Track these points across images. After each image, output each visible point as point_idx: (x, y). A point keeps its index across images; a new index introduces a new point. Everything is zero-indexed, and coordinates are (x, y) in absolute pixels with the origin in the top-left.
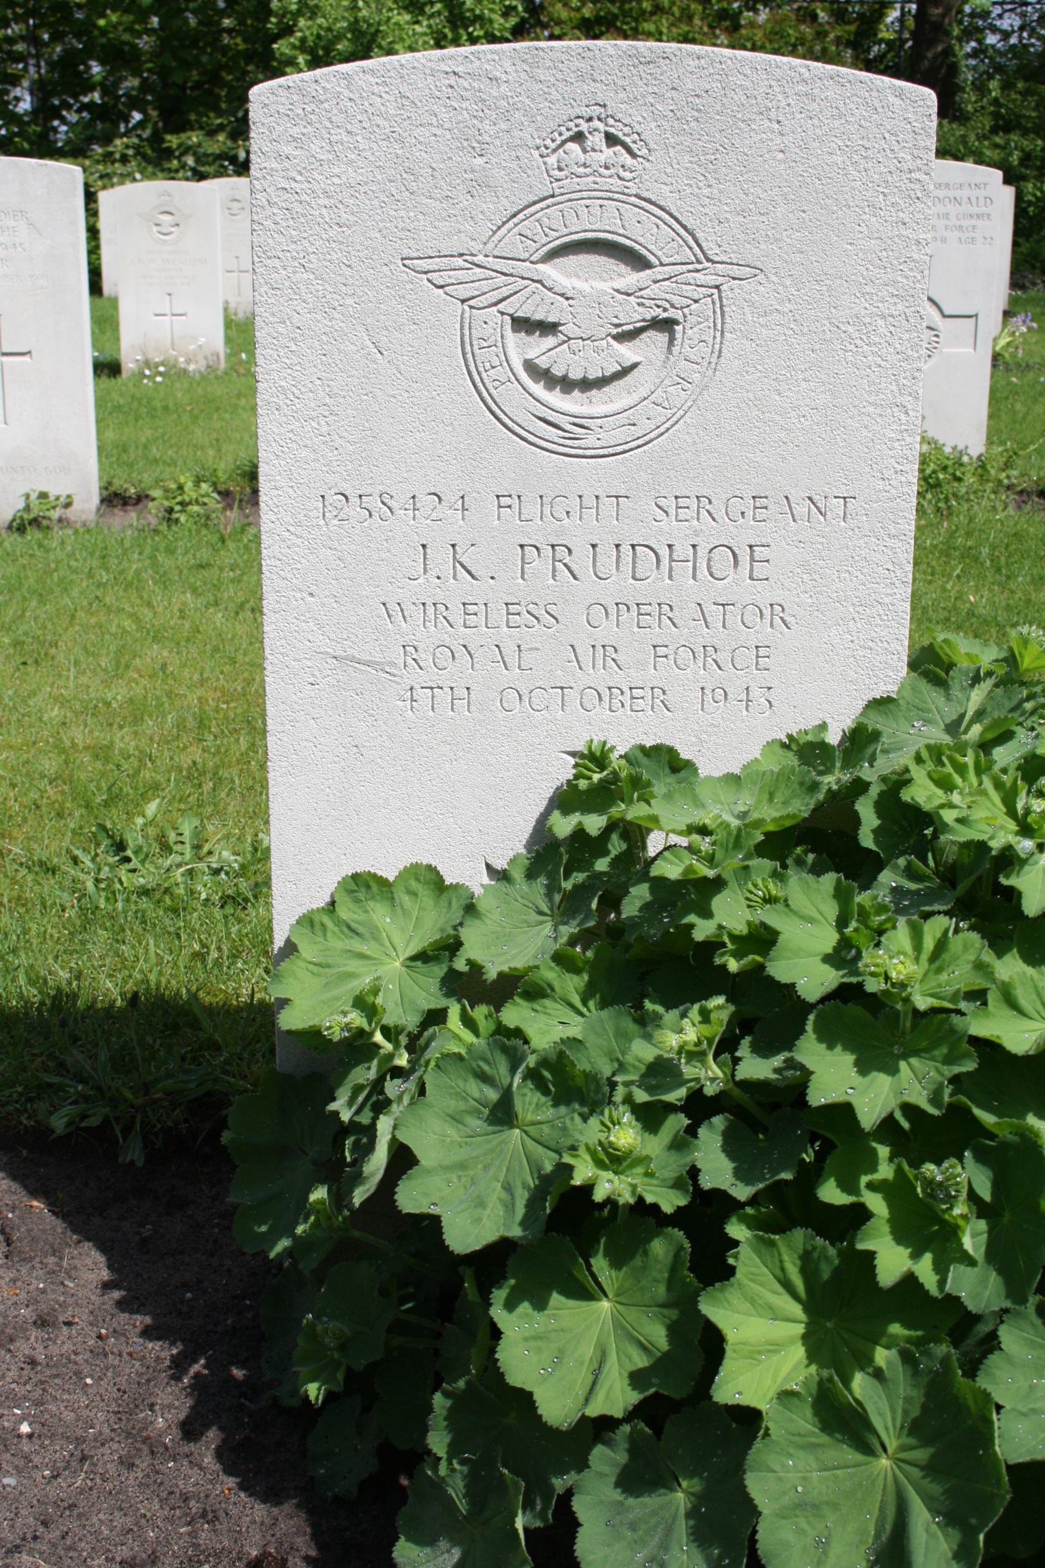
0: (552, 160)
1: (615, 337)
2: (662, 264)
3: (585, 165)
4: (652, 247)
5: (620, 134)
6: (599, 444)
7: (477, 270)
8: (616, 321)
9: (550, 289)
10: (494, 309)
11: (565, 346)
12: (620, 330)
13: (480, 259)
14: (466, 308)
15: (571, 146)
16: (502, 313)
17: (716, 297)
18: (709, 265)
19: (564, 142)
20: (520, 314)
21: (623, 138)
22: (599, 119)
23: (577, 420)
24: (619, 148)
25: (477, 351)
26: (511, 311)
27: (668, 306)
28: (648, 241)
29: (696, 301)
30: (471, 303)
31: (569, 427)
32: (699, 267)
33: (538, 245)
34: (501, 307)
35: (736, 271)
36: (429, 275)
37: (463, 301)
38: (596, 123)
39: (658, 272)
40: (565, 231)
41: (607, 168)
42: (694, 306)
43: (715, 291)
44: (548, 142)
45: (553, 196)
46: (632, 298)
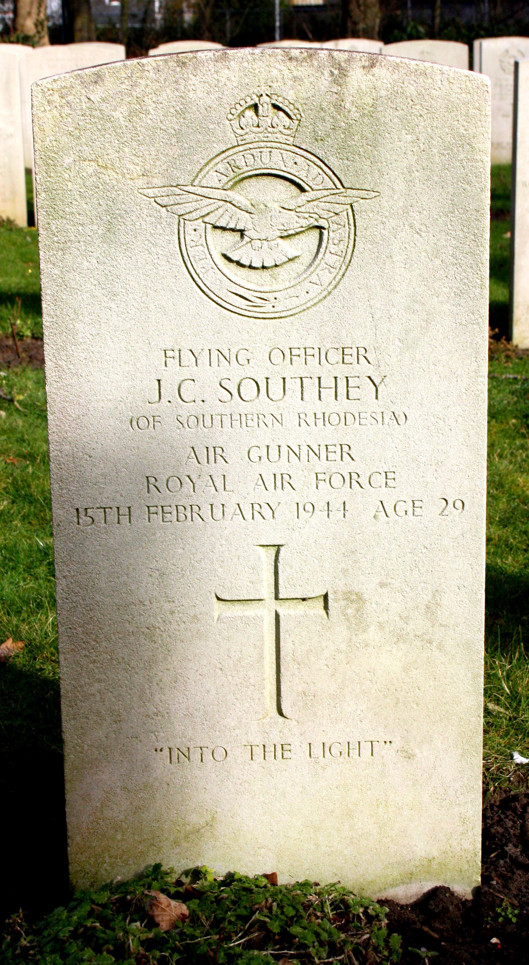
4: (305, 179)
5: (281, 105)
9: (239, 208)
10: (200, 221)
17: (350, 211)
18: (343, 190)
19: (243, 111)
20: (218, 224)
22: (267, 95)
23: (259, 295)
24: (281, 114)
27: (317, 217)
28: (303, 175)
29: (336, 214)
30: (184, 217)
32: (338, 191)
34: (206, 219)
35: (363, 194)
36: (156, 199)
38: (265, 98)
39: (310, 195)
40: (246, 169)
43: (348, 207)
44: (233, 111)
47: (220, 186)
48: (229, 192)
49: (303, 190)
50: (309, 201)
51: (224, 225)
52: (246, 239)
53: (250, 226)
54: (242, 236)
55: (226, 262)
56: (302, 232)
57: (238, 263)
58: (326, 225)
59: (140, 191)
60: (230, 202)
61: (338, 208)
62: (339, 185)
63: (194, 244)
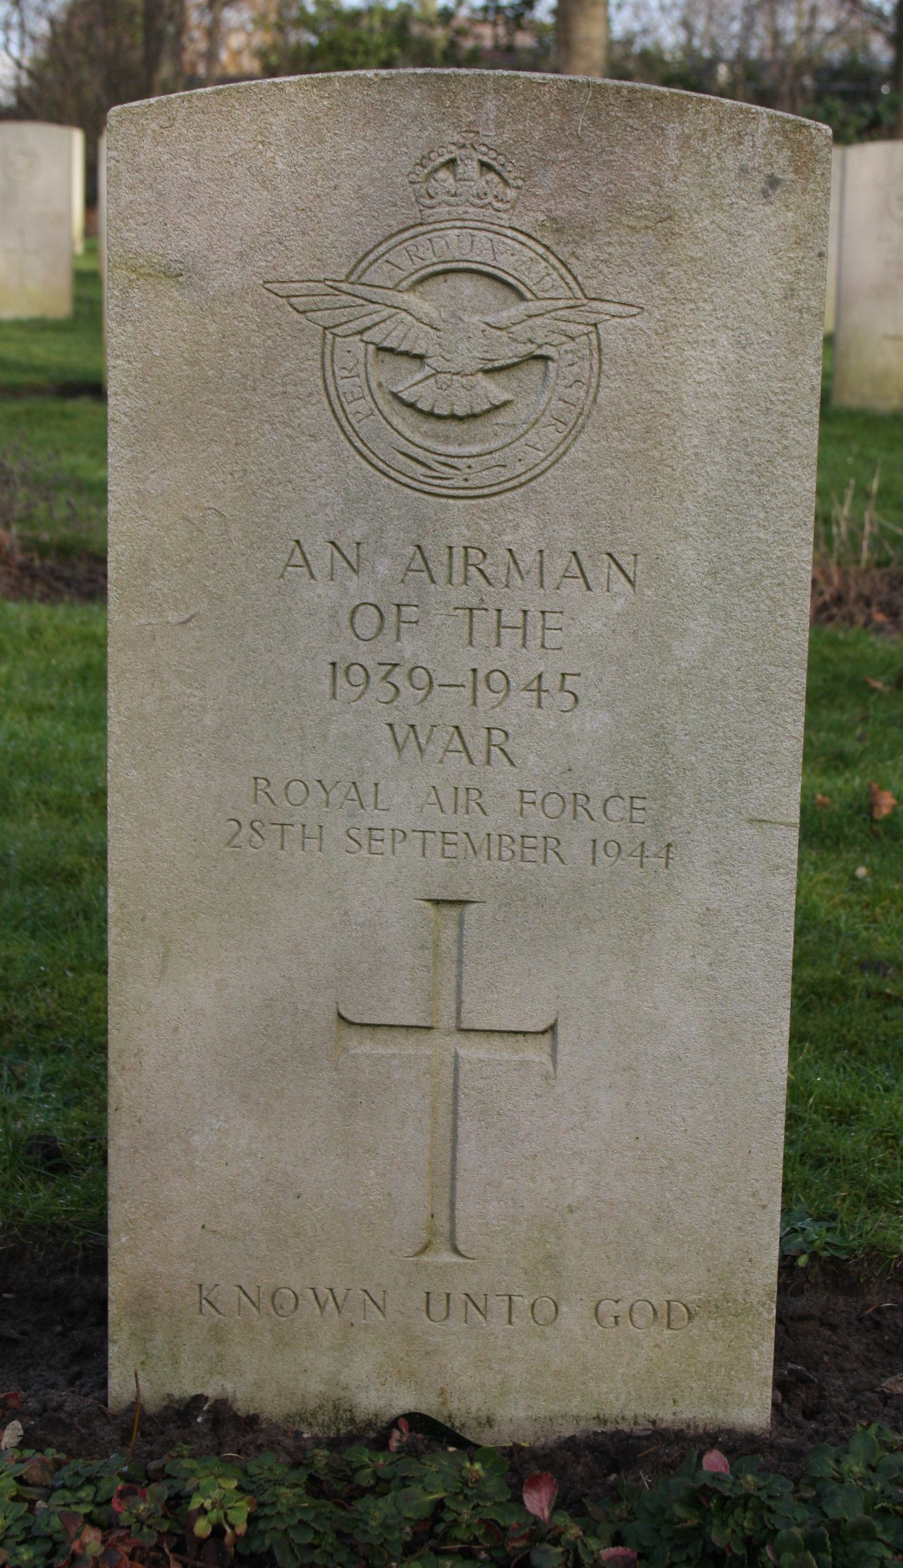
0: (421, 188)
1: (486, 372)
2: (538, 299)
3: (455, 195)
6: (467, 484)
7: (344, 297)
8: (488, 356)
10: (358, 337)
11: (432, 380)
12: (490, 366)
13: (344, 286)
14: (330, 336)
15: (442, 174)
16: (367, 343)
17: (593, 337)
18: (585, 301)
20: (385, 344)
21: (498, 168)
23: (442, 459)
25: (340, 382)
26: (377, 340)
30: (334, 331)
31: (435, 465)
33: (405, 274)
37: (326, 328)
39: (534, 307)
41: (479, 197)
42: (572, 344)
43: (591, 328)
45: (421, 224)
46: (504, 333)
47: (390, 284)
48: (405, 296)
49: (522, 297)
50: (530, 316)
51: (394, 345)
52: (428, 371)
53: (434, 350)
54: (423, 364)
55: (396, 405)
56: (514, 365)
57: (411, 406)
58: (556, 357)
59: (267, 286)
60: (405, 310)
61: (572, 328)
62: (579, 294)
63: (346, 373)
